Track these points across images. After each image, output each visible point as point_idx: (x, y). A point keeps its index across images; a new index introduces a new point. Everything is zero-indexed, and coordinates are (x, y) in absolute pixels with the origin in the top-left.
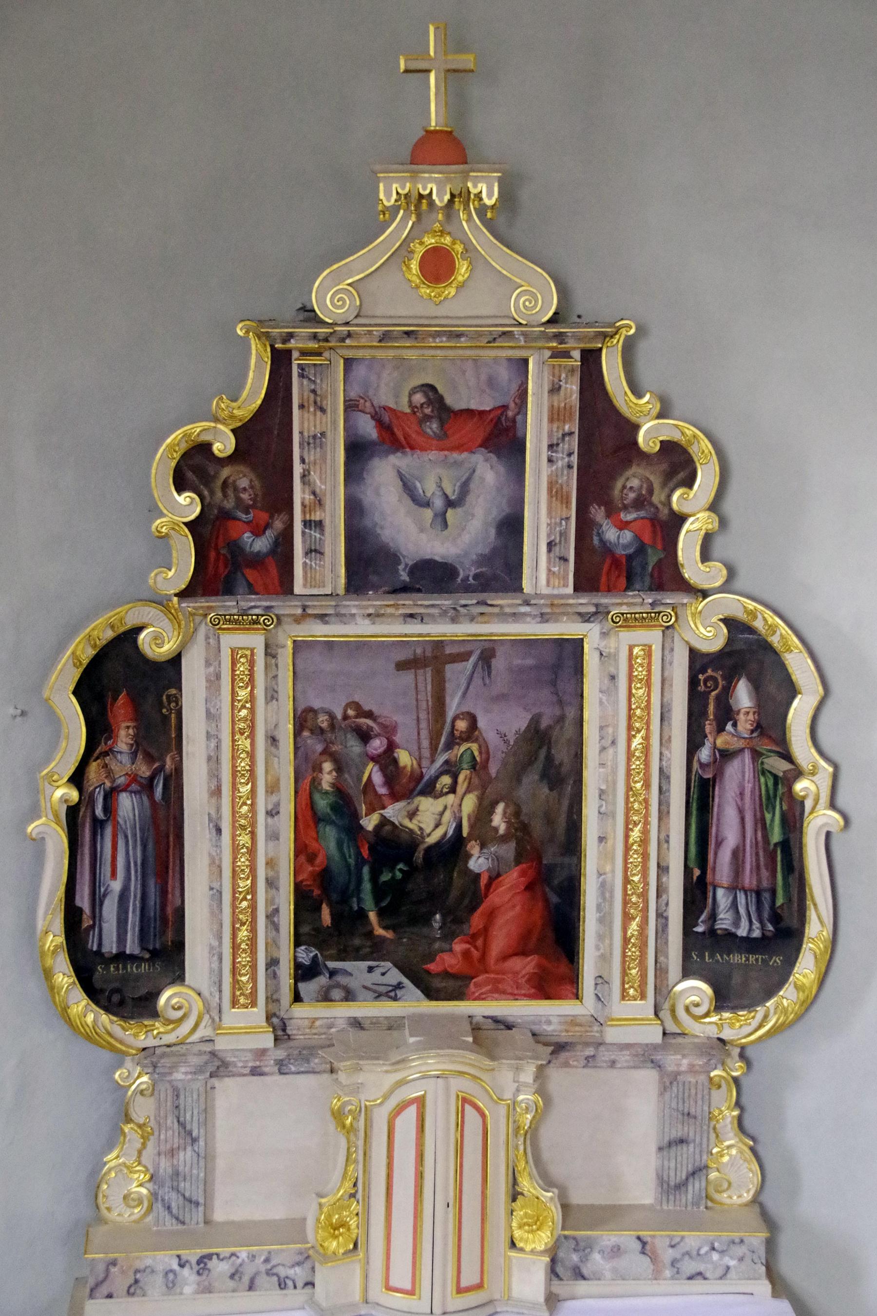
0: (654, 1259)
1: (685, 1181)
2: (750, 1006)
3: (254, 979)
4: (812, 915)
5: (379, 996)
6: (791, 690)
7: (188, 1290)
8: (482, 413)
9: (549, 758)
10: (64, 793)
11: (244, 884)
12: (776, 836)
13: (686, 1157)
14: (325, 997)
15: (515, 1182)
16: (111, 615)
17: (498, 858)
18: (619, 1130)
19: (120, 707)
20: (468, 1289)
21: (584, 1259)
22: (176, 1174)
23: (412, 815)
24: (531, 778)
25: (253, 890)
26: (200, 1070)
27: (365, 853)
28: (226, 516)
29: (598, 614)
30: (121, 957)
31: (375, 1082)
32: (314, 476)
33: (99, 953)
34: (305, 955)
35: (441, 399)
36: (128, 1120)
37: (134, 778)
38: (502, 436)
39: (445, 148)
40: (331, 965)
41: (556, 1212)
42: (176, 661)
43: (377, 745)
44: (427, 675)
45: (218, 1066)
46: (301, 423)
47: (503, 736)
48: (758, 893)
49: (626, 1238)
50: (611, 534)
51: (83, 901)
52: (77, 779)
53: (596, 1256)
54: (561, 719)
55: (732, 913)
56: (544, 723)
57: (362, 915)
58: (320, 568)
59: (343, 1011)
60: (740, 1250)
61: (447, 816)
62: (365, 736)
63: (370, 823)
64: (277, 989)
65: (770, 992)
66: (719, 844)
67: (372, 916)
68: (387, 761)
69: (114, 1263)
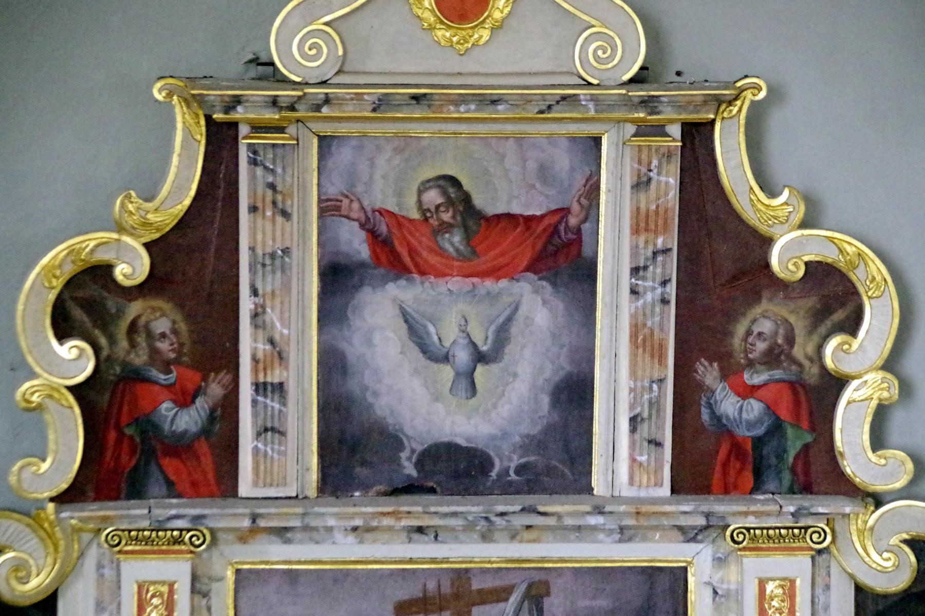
8: (529, 220)
28: (134, 377)
29: (712, 528)
32: (272, 315)
35: (467, 199)
38: (559, 253)
50: (729, 405)
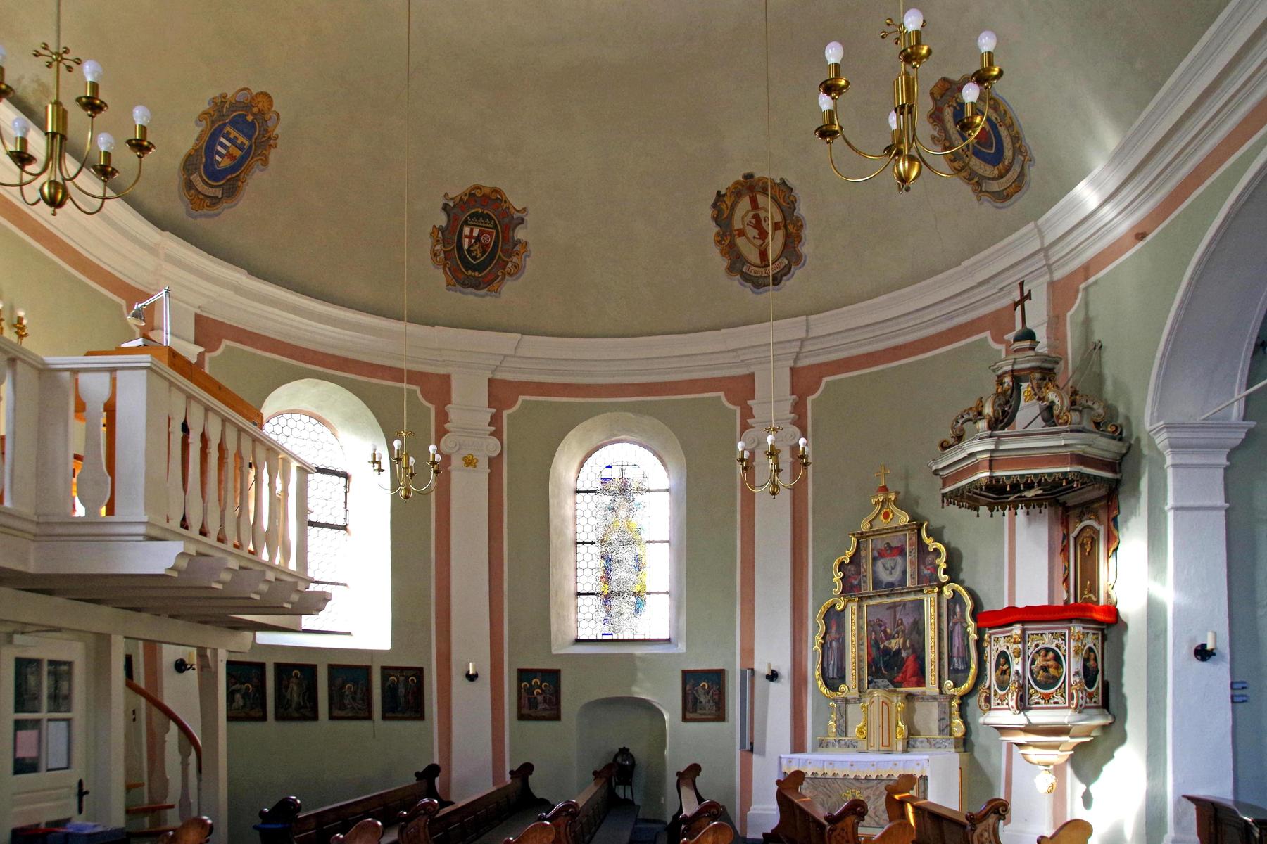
18: (928, 716)
38: (901, 551)
46: (863, 553)
52: (824, 638)
55: (958, 664)
68: (885, 631)
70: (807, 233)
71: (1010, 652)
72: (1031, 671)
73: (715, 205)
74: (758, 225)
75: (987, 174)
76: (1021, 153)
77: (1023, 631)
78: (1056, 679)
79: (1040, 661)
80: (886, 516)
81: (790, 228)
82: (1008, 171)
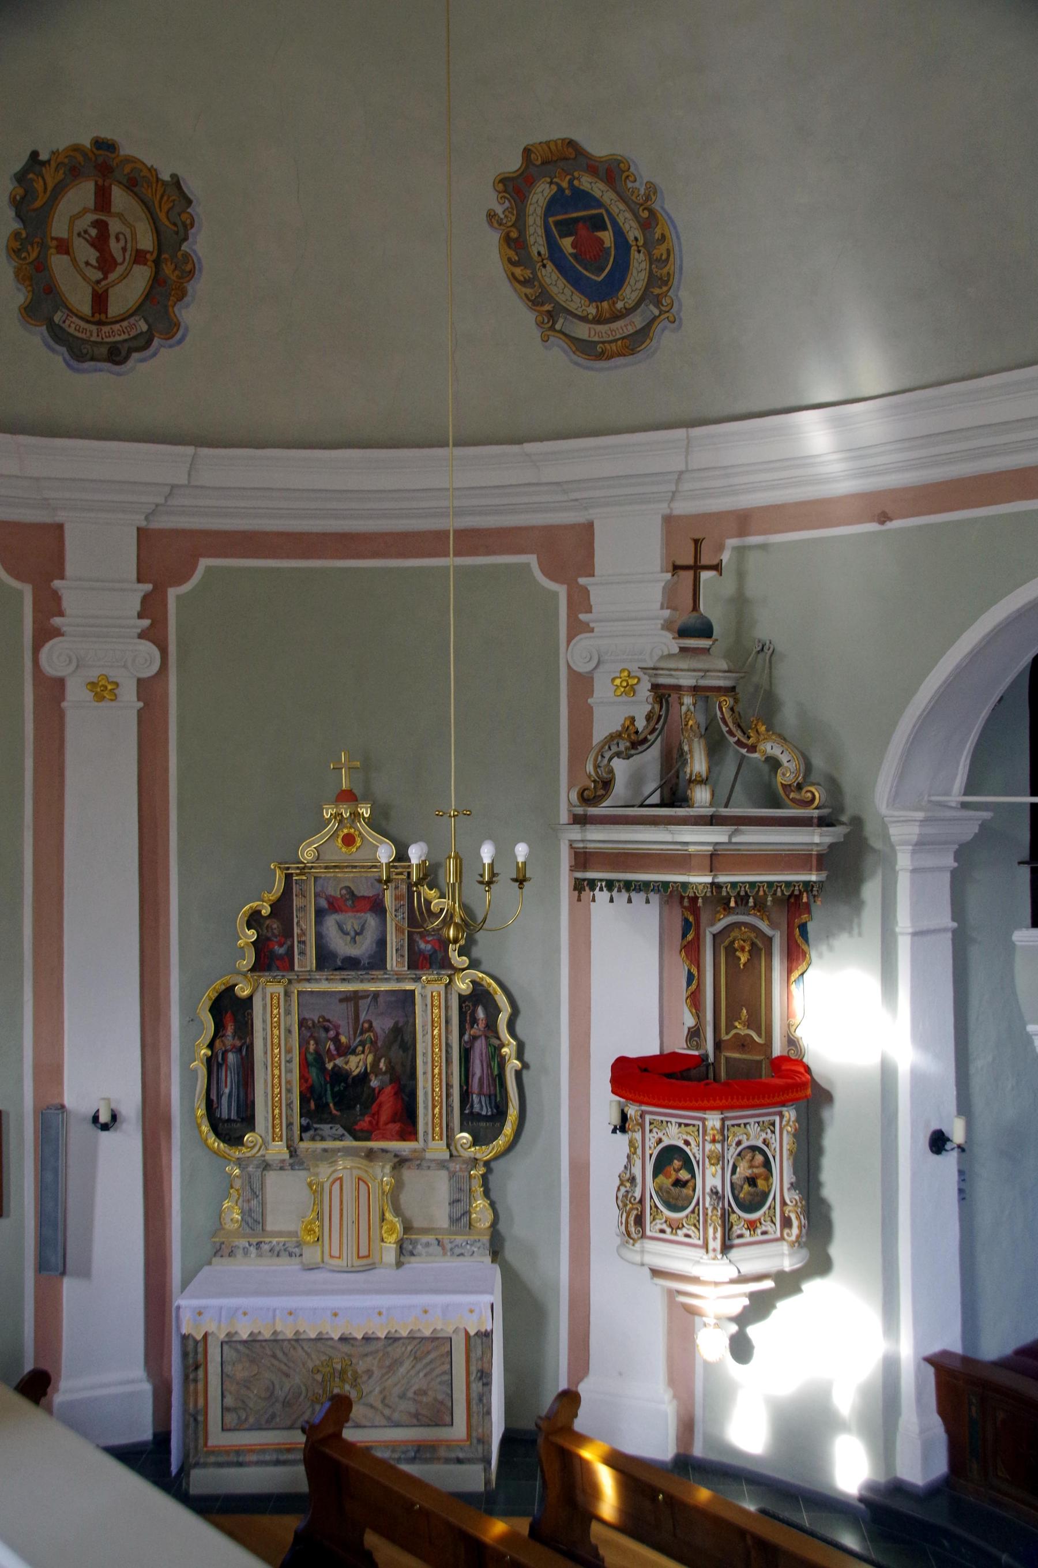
0: (444, 1248)
1: (461, 1219)
2: (487, 1144)
3: (281, 1130)
4: (510, 1104)
5: (335, 1139)
6: (499, 1011)
7: (253, 1256)
8: (369, 898)
9: (402, 1040)
10: (204, 1051)
11: (277, 1091)
12: (496, 1072)
13: (459, 1209)
14: (313, 1139)
15: (383, 1215)
16: (225, 979)
17: (382, 1081)
18: (431, 1196)
19: (228, 1017)
20: (363, 1257)
21: (414, 1247)
22: (250, 1210)
23: (347, 1063)
24: (395, 1047)
25: (280, 1093)
26: (258, 1167)
27: (328, 1079)
28: (268, 939)
29: (417, 979)
30: (229, 1120)
31: (324, 1171)
32: (301, 923)
33: (220, 1118)
34: (304, 1122)
35: (352, 892)
36: (232, 1187)
37: (234, 1046)
38: (377, 907)
39: (348, 797)
40: (316, 1126)
41: (399, 1227)
42: (250, 998)
43: (332, 1034)
44: (351, 1004)
45: (266, 1166)
46: (297, 902)
47: (383, 1030)
48: (490, 1097)
49: (430, 1238)
50: (422, 946)
51: (214, 1097)
52: (211, 1046)
53: (419, 1247)
54: (407, 1023)
55: (480, 1105)
56: (400, 1025)
57: (327, 1104)
58: (306, 960)
59: (320, 1145)
60: (478, 1244)
61: (361, 1064)
62: (327, 1030)
63: (330, 1066)
64: (293, 1135)
65: (496, 1138)
66: (473, 1076)
67: (331, 1105)
68: (336, 1040)
69: (223, 1243)
70: (199, 287)
71: (693, 1151)
72: (732, 1184)
73: (21, 178)
74: (101, 241)
75: (572, 307)
76: (658, 303)
77: (723, 1120)
78: (765, 1195)
79: (743, 1170)
80: (349, 840)
81: (167, 269)
82: (616, 317)
